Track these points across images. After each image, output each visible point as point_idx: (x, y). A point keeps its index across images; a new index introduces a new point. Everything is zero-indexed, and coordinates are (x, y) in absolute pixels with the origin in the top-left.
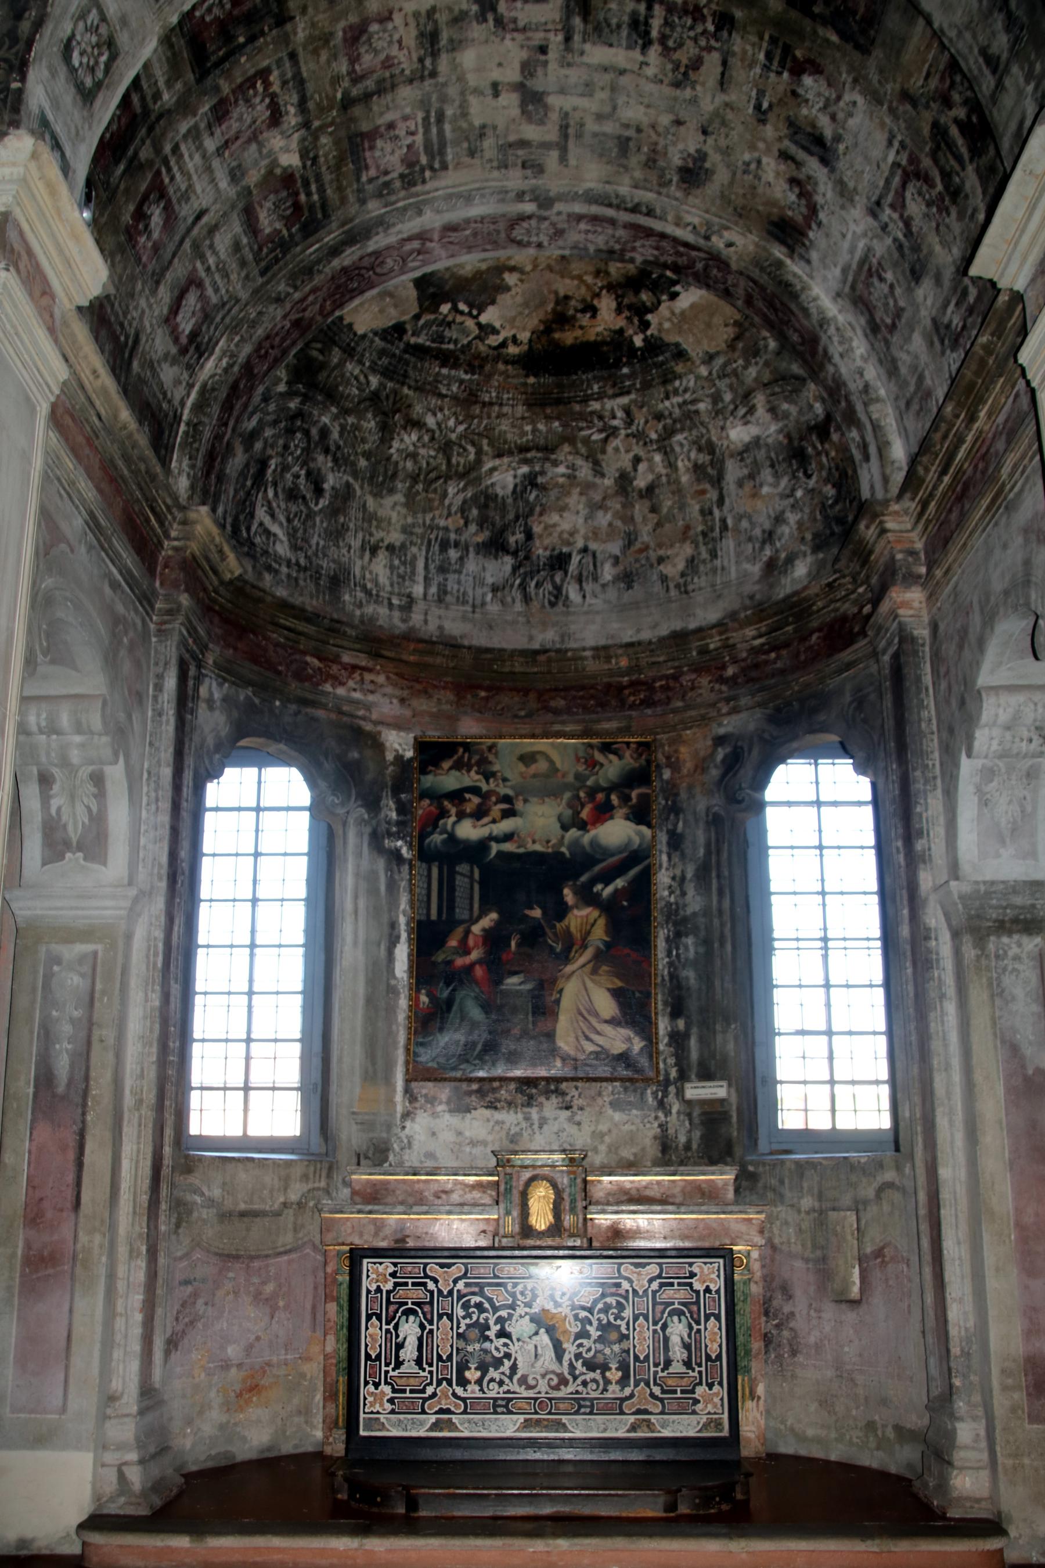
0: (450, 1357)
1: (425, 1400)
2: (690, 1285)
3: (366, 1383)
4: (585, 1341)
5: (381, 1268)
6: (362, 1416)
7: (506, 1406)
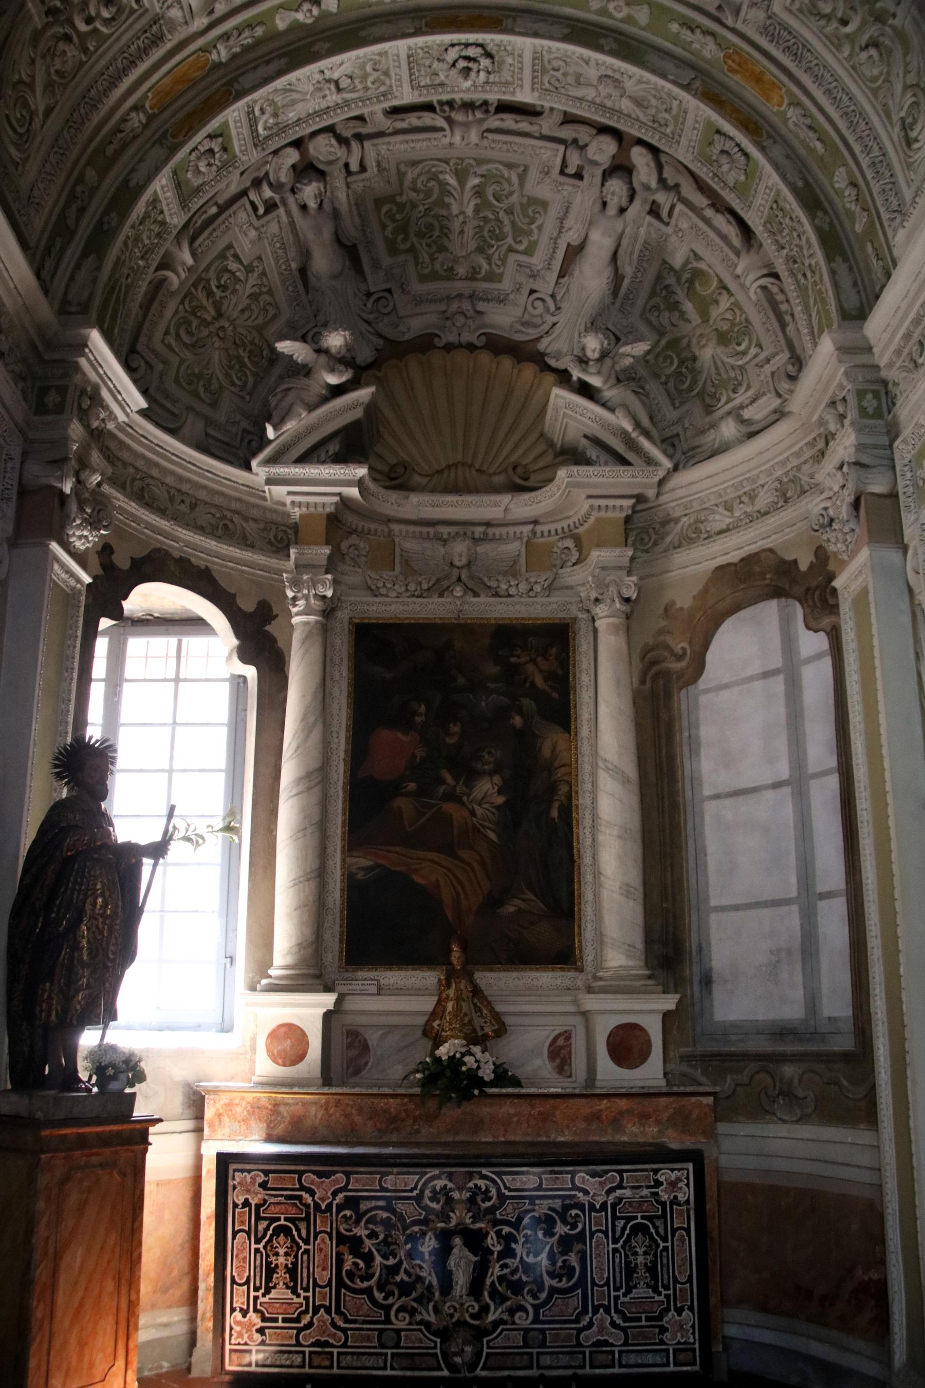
3: (233, 1310)
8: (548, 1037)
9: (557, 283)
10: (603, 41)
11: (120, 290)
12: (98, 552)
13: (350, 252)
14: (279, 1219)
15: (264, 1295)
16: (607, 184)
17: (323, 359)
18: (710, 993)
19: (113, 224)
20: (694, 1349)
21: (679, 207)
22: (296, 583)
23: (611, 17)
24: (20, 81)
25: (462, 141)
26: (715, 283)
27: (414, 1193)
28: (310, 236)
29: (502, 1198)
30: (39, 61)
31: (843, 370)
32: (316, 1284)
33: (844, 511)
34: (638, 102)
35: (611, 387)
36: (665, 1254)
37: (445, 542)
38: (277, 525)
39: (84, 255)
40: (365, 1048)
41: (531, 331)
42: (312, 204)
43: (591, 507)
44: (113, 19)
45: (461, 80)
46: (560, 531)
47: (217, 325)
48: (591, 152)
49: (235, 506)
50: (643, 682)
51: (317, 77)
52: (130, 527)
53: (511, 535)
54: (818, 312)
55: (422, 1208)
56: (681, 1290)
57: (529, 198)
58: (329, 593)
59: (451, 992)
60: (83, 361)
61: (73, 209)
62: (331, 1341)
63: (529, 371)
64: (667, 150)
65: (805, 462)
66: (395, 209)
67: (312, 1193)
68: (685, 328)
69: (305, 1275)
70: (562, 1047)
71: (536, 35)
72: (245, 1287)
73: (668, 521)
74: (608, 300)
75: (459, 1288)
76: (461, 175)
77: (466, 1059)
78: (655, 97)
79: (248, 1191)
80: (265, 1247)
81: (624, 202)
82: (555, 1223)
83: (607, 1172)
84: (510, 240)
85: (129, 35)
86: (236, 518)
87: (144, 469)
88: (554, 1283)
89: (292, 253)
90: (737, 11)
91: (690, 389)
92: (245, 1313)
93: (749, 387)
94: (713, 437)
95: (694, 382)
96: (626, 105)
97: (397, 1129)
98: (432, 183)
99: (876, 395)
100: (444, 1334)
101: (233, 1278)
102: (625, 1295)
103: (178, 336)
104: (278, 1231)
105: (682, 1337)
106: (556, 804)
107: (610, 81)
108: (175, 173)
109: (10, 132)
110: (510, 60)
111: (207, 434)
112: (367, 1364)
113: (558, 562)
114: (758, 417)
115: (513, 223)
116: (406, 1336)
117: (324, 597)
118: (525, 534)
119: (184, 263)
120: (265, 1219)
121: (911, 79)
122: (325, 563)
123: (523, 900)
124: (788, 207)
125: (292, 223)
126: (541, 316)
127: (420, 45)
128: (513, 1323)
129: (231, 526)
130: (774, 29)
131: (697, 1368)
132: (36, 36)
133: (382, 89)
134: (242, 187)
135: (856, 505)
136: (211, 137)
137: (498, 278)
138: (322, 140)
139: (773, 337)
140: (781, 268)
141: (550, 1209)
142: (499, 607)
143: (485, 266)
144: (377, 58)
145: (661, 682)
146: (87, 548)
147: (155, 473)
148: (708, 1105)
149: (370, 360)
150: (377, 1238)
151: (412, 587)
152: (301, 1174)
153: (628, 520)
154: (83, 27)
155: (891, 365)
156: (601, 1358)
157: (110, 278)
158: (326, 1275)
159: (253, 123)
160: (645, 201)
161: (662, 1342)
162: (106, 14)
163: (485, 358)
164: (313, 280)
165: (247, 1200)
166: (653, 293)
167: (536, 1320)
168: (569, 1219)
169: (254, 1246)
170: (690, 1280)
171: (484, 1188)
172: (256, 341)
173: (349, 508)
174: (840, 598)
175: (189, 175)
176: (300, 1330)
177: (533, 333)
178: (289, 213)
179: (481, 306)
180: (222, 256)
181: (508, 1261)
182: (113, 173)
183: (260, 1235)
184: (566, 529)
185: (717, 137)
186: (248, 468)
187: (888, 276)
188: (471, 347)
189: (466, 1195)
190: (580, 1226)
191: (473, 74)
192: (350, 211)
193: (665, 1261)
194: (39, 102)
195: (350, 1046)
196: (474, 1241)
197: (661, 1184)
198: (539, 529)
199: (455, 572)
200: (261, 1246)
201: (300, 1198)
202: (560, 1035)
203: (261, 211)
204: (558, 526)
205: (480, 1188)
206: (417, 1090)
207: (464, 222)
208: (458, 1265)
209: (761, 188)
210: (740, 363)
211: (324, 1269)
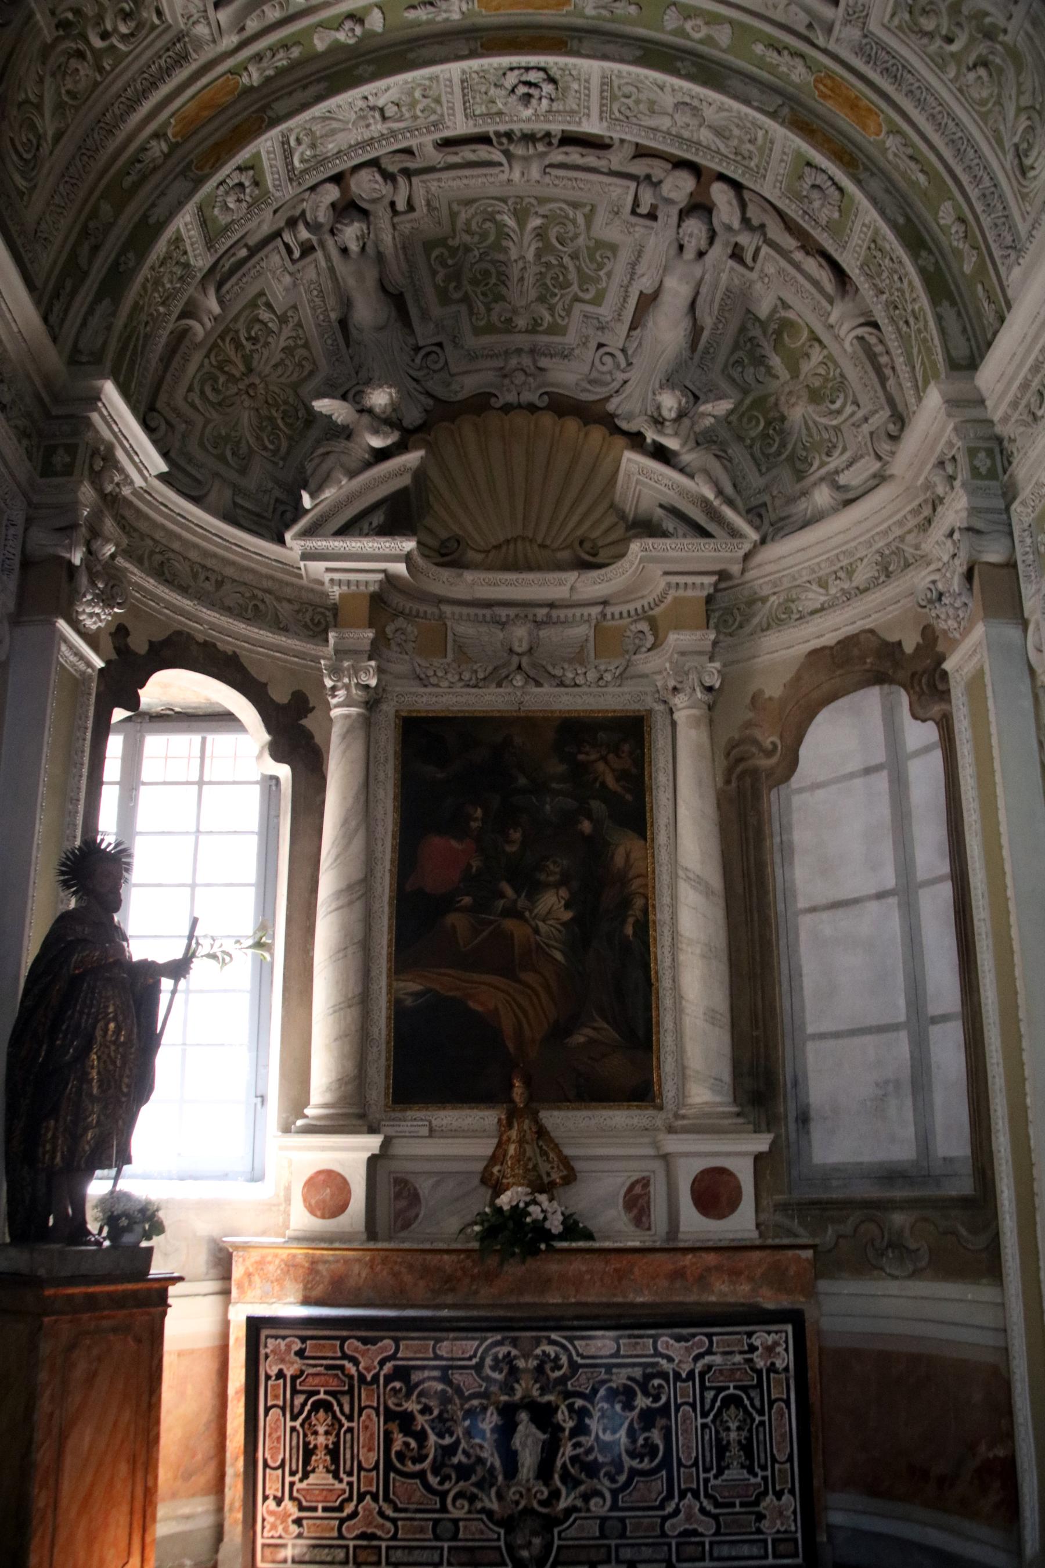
3: (265, 1498)
8: (623, 1184)
9: (628, 336)
10: (679, 64)
11: (137, 339)
12: (111, 634)
13: (396, 300)
14: (318, 1393)
15: (301, 1480)
16: (684, 225)
17: (366, 419)
18: (808, 1133)
19: (131, 264)
20: (796, 1540)
21: (765, 250)
22: (336, 671)
23: (687, 36)
24: (27, 101)
25: (521, 176)
26: (805, 334)
27: (474, 1361)
28: (351, 282)
29: (574, 1367)
30: (48, 80)
31: (952, 426)
32: (360, 1468)
33: (956, 583)
34: (719, 132)
35: (691, 450)
36: (761, 1429)
37: (503, 625)
38: (315, 606)
39: (98, 299)
40: (415, 1198)
41: (598, 389)
42: (354, 247)
43: (669, 584)
44: (132, 35)
45: (521, 108)
46: (633, 613)
47: (247, 381)
48: (666, 189)
49: (267, 584)
50: (728, 782)
51: (361, 103)
52: (146, 605)
53: (578, 618)
54: (923, 363)
55: (483, 1379)
56: (780, 1470)
57: (597, 241)
58: (373, 682)
59: (514, 1134)
60: (95, 417)
61: (86, 247)
62: (379, 1533)
63: (597, 434)
64: (751, 185)
65: (910, 532)
66: (446, 253)
67: (355, 1362)
68: (774, 385)
69: (348, 1456)
70: (640, 1196)
71: (605, 57)
72: (280, 1471)
73: (754, 600)
74: (686, 354)
75: (525, 1470)
76: (521, 215)
77: (532, 1209)
78: (738, 126)
79: (282, 1361)
80: (302, 1425)
81: (703, 244)
82: (635, 1394)
83: (694, 1335)
84: (575, 288)
85: (149, 53)
86: (268, 598)
87: (164, 541)
88: (635, 1463)
89: (331, 302)
90: (829, 29)
91: (779, 453)
92: (279, 1501)
93: (844, 449)
94: (804, 506)
95: (783, 445)
96: (705, 135)
97: (453, 1290)
98: (488, 225)
99: (990, 452)
100: (509, 1524)
101: (265, 1461)
102: (716, 1477)
103: (202, 392)
104: (317, 1406)
105: (782, 1524)
106: (631, 920)
107: (687, 109)
108: (200, 209)
109: (15, 158)
110: (575, 86)
111: (235, 504)
112: (420, 1559)
113: (631, 647)
114: (855, 482)
115: (579, 269)
116: (465, 1527)
117: (367, 687)
118: (594, 616)
119: (210, 312)
120: (302, 1392)
121: (1026, 100)
122: (368, 648)
123: (594, 1029)
124: (888, 247)
125: (332, 269)
126: (610, 373)
127: (476, 68)
128: (588, 1510)
129: (262, 606)
130: (870, 48)
131: (799, 1560)
132: (46, 50)
133: (433, 118)
134: (275, 227)
135: (969, 576)
136: (240, 169)
137: (562, 331)
138: (365, 175)
139: (872, 393)
140: (880, 316)
141: (630, 1378)
142: (564, 698)
143: (548, 318)
144: (427, 82)
145: (748, 780)
146: (99, 628)
147: (176, 546)
148: (807, 1260)
149: (420, 422)
150: (431, 1413)
151: (466, 676)
152: (343, 1340)
153: (709, 599)
154: (98, 43)
155: (1005, 419)
156: (690, 1550)
157: (126, 326)
158: (373, 1457)
159: (288, 154)
160: (726, 244)
161: (759, 1531)
162: (124, 29)
163: (547, 419)
164: (354, 332)
165: (281, 1371)
166: (736, 347)
167: (614, 1507)
168: (652, 1391)
169: (289, 1424)
170: (790, 1459)
171: (553, 1355)
172: (291, 400)
173: (395, 587)
174: (952, 683)
175: (216, 211)
176: (342, 1521)
177: (601, 392)
178: (328, 258)
179: (543, 362)
180: (253, 304)
181: (582, 1439)
182: (129, 210)
183: (296, 1410)
184: (640, 611)
185: (807, 170)
186: (281, 541)
187: (1002, 320)
188: (532, 408)
189: (533, 1363)
190: (664, 1399)
191: (534, 102)
192: (397, 256)
193: (761, 1437)
194: (48, 126)
195: (398, 1196)
196: (543, 1416)
197: (757, 1349)
198: (609, 610)
199: (515, 660)
200: (297, 1424)
201: (342, 1368)
202: (637, 1182)
203: (297, 254)
204: (631, 607)
205: (549, 1356)
206: (475, 1245)
207: (524, 268)
208: (524, 1445)
209: (857, 227)
210: (834, 423)
211: (370, 1450)
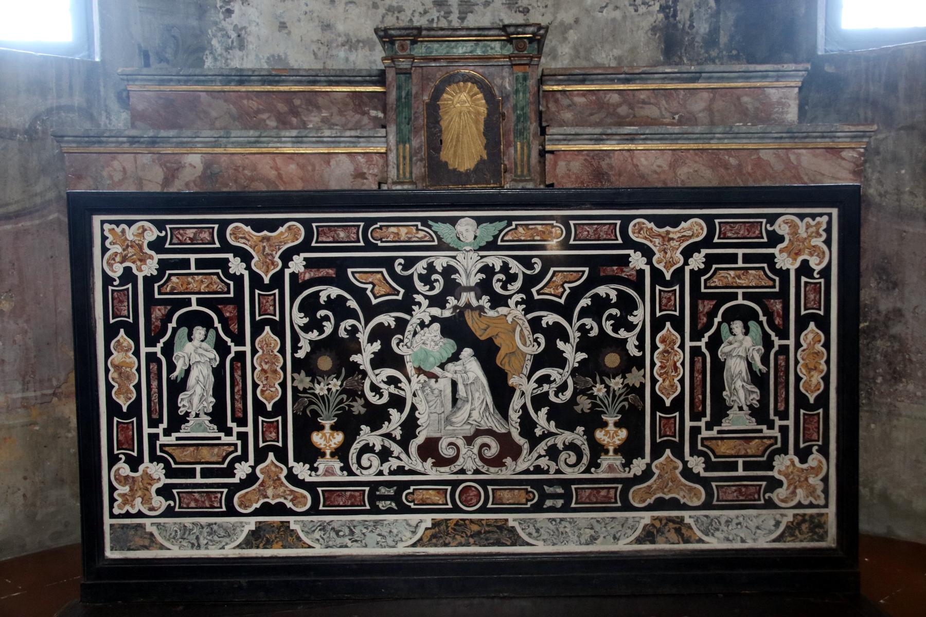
0: (280, 407)
1: (233, 489)
2: (770, 259)
3: (113, 460)
4: (554, 373)
5: (131, 233)
6: (107, 521)
7: (396, 498)
62: (289, 505)
